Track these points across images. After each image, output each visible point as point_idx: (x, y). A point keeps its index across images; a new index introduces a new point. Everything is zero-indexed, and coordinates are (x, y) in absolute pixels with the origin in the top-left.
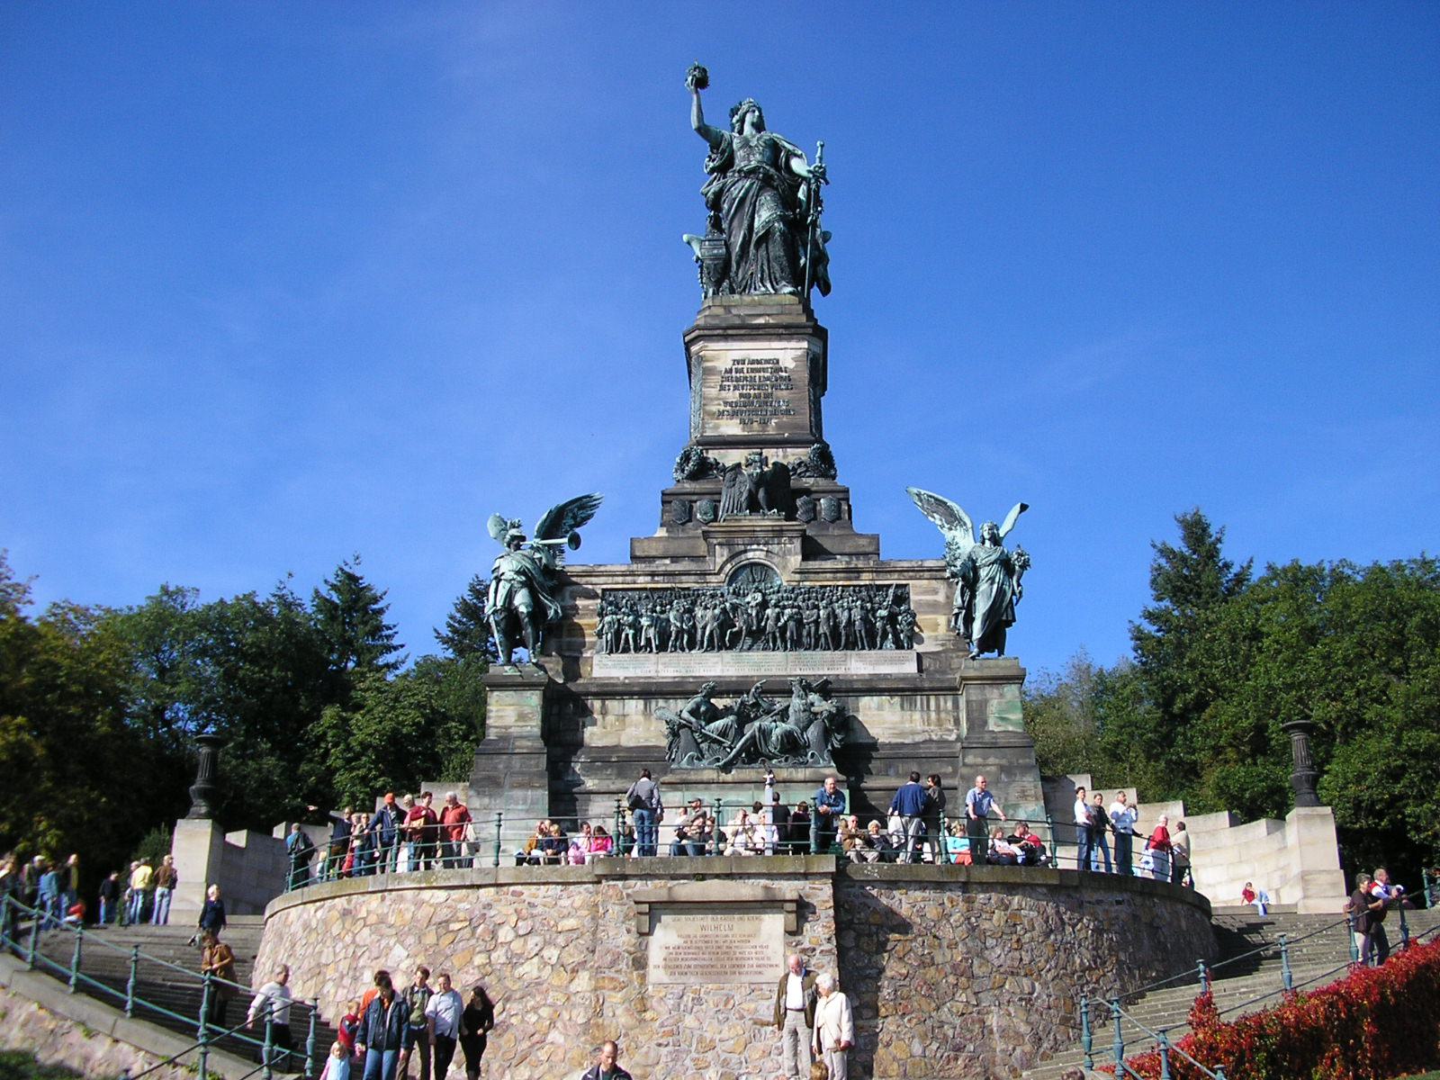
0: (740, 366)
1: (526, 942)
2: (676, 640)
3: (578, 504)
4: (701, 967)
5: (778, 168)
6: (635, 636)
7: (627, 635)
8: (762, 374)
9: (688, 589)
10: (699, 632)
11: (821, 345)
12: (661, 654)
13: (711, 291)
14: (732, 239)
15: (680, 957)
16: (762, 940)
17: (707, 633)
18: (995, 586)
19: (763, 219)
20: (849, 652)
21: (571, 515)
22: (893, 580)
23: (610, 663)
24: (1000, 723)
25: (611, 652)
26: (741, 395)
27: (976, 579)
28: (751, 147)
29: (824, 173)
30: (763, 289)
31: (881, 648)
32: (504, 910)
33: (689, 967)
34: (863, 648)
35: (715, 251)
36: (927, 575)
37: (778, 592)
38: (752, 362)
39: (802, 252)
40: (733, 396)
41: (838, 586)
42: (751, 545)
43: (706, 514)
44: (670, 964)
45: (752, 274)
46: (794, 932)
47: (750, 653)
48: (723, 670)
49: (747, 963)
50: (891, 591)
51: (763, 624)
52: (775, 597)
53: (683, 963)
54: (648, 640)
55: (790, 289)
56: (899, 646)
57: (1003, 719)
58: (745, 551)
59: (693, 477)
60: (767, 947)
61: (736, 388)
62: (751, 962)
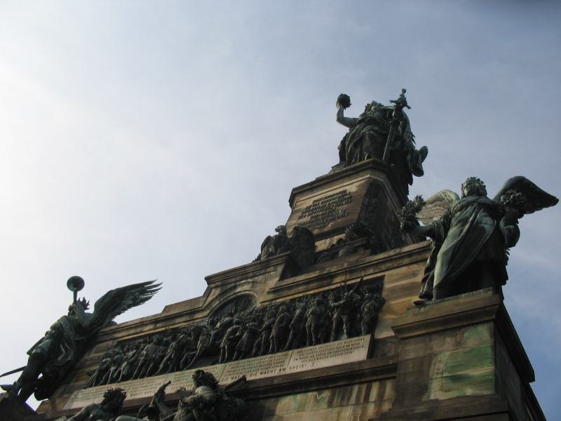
6: (116, 370)
20: (290, 352)
21: (132, 297)
22: (370, 275)
24: (451, 385)
26: (311, 218)
34: (311, 344)
36: (406, 261)
54: (120, 371)
56: (351, 334)
57: (455, 379)
58: (235, 287)
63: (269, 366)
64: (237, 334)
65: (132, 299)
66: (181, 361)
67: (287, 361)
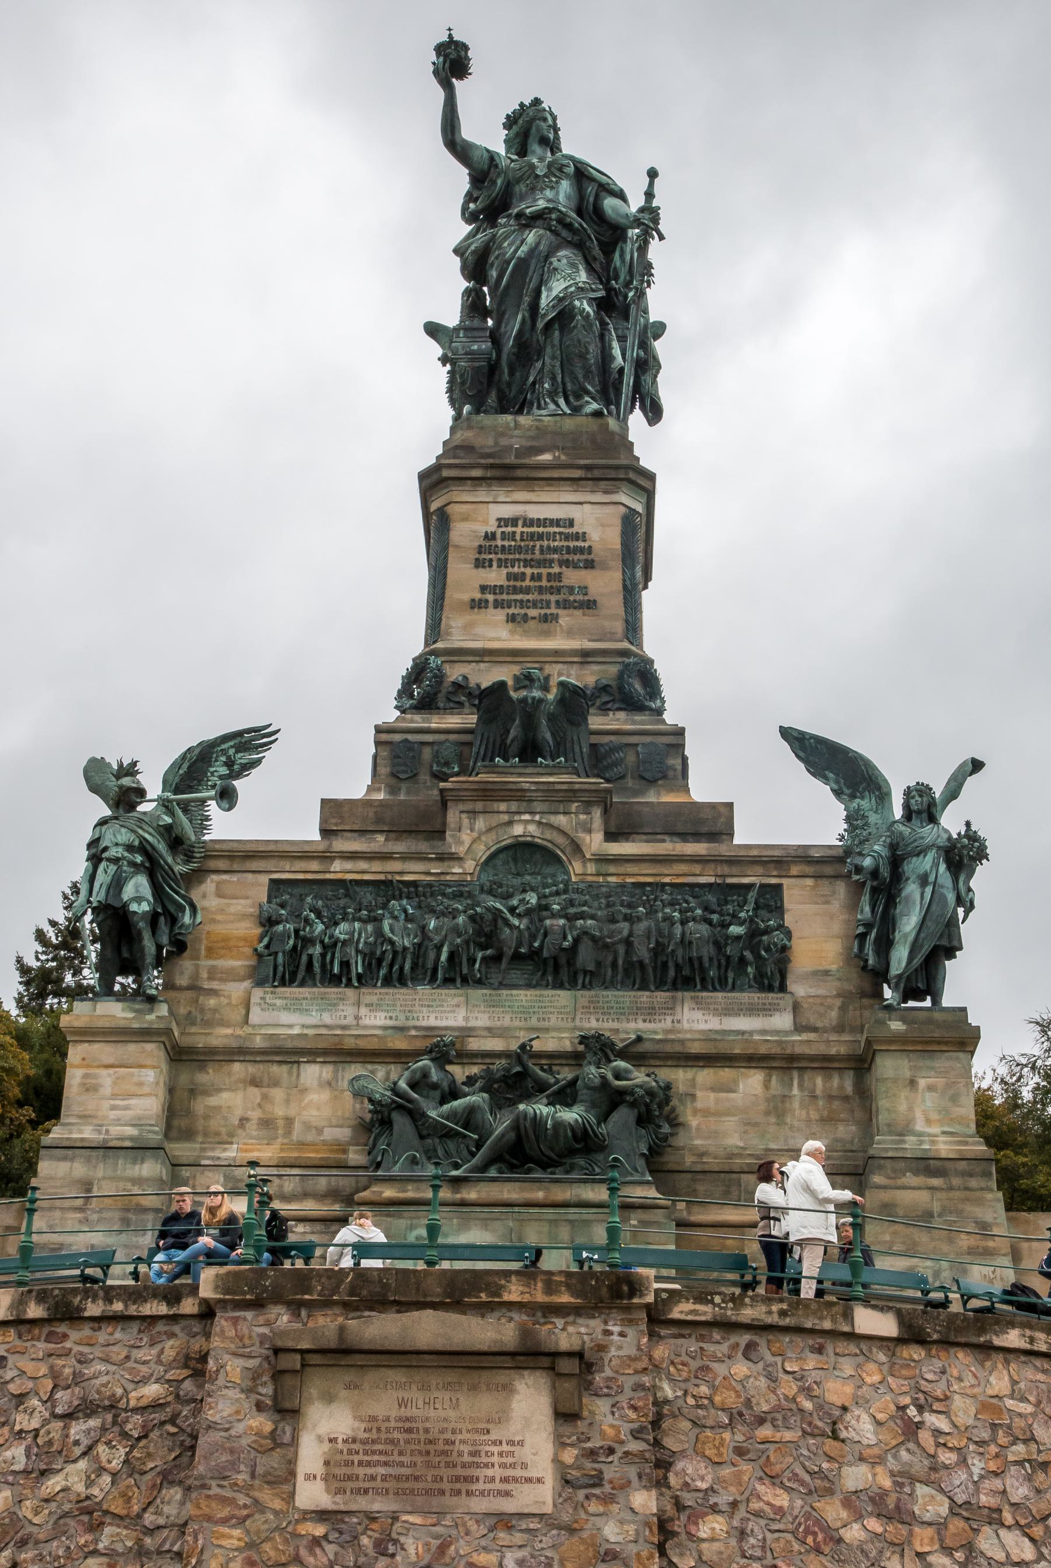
0: (510, 529)
1: (66, 1427)
2: (391, 966)
3: (237, 741)
4: (398, 1478)
5: (579, 212)
6: (323, 956)
7: (310, 957)
8: (545, 543)
9: (414, 884)
10: (432, 955)
11: (644, 500)
12: (363, 990)
13: (467, 408)
14: (503, 329)
15: (356, 1458)
16: (512, 1429)
17: (444, 957)
18: (929, 890)
19: (554, 293)
20: (679, 994)
21: (223, 759)
23: (278, 1002)
25: (283, 984)
26: (510, 576)
27: (897, 877)
28: (537, 176)
29: (656, 220)
30: (552, 406)
31: (733, 989)
32: (29, 1367)
33: (373, 1478)
34: (704, 988)
35: (475, 347)
37: (566, 891)
38: (529, 522)
39: (617, 351)
40: (496, 576)
41: (664, 885)
42: (519, 813)
43: (447, 764)
44: (337, 1471)
45: (534, 383)
46: (565, 1415)
47: (514, 992)
48: (466, 1019)
49: (481, 1473)
50: (752, 896)
51: (536, 945)
52: (557, 899)
53: (361, 1471)
54: (345, 965)
55: (595, 406)
58: (510, 823)
59: (426, 705)
60: (521, 1443)
61: (501, 563)
62: (490, 1472)
63: (651, 1013)
64: (570, 938)
65: (226, 764)
66: (477, 966)
67: (679, 1009)
